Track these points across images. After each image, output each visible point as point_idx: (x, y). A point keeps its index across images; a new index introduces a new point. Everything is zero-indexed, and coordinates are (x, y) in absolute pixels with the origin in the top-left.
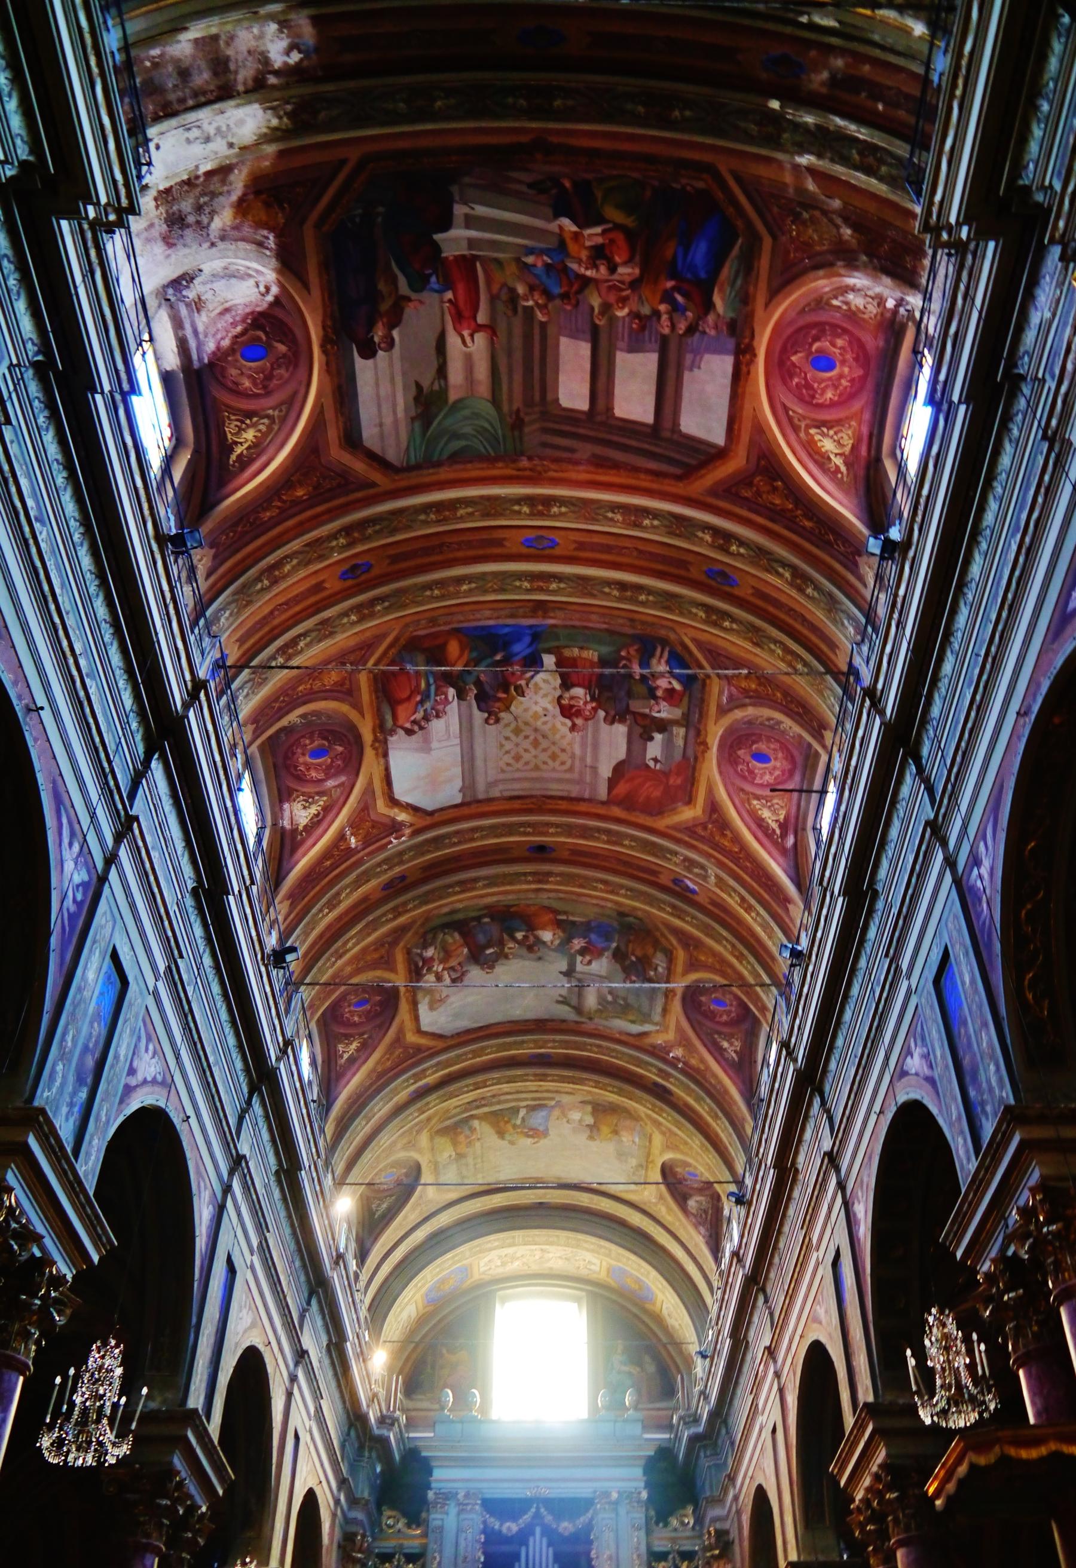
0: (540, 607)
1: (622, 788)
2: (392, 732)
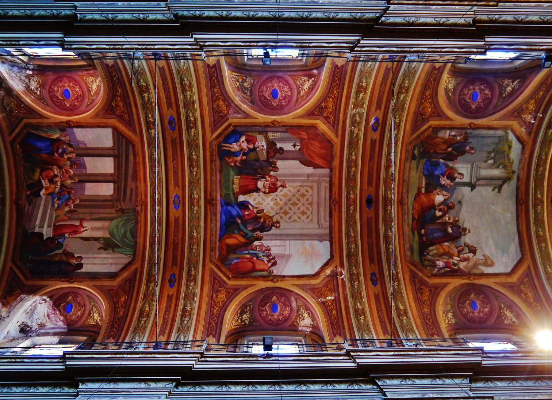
0: (210, 202)
1: (318, 161)
2: (271, 272)
